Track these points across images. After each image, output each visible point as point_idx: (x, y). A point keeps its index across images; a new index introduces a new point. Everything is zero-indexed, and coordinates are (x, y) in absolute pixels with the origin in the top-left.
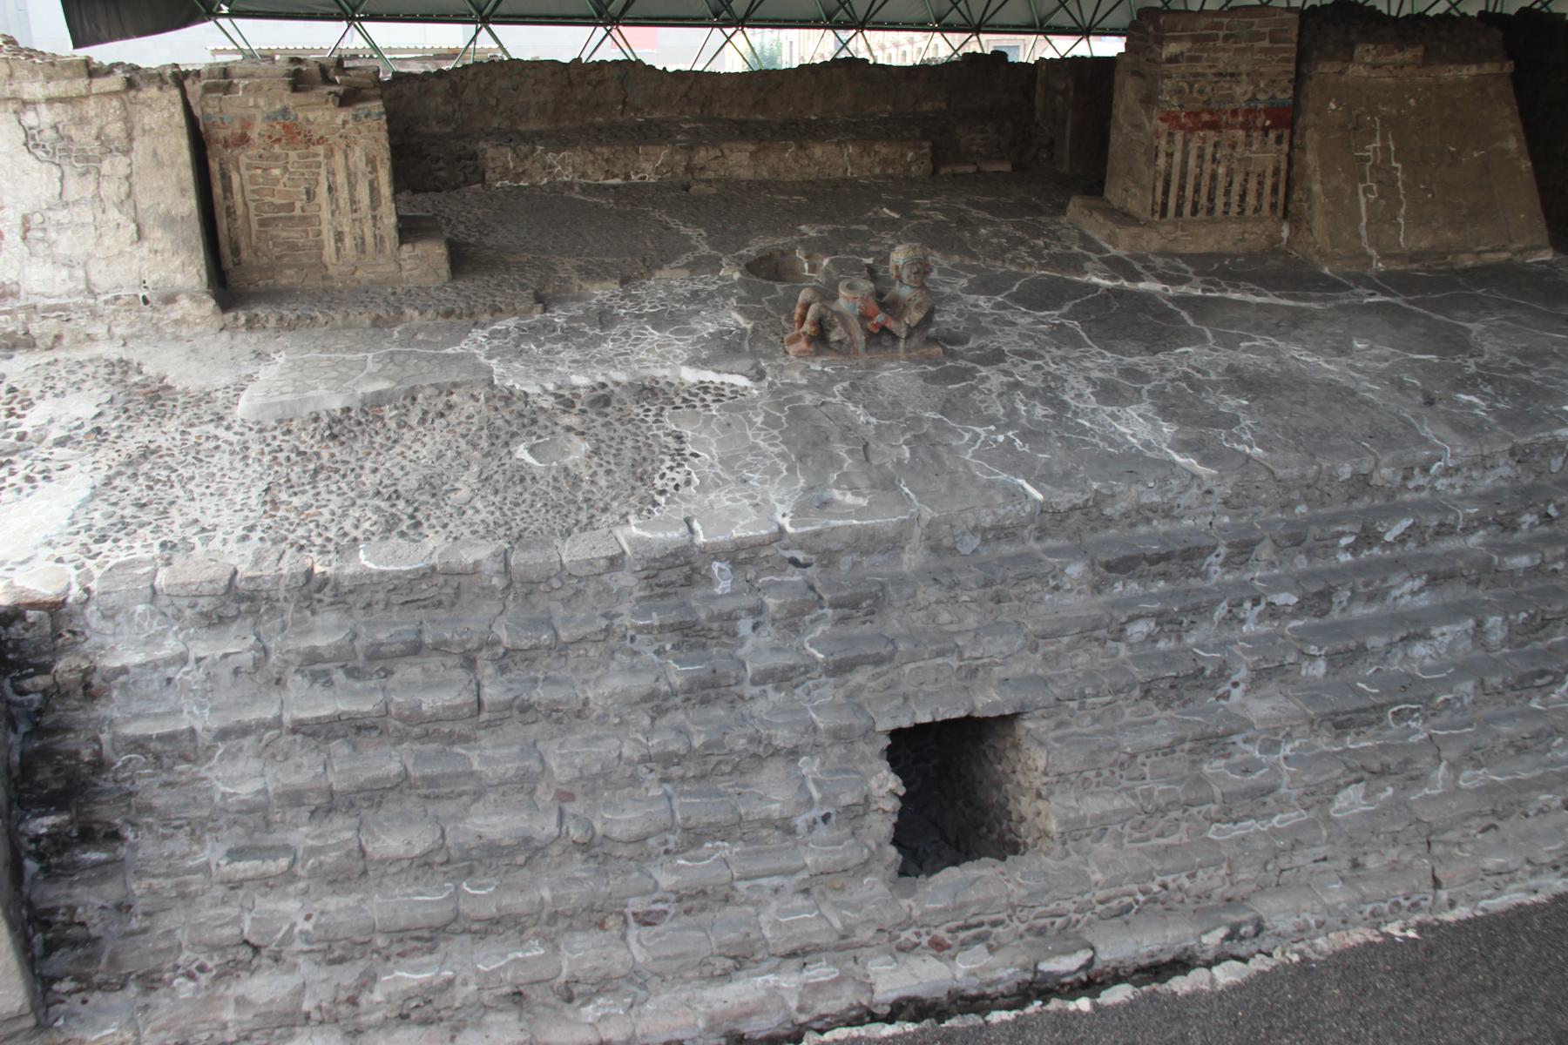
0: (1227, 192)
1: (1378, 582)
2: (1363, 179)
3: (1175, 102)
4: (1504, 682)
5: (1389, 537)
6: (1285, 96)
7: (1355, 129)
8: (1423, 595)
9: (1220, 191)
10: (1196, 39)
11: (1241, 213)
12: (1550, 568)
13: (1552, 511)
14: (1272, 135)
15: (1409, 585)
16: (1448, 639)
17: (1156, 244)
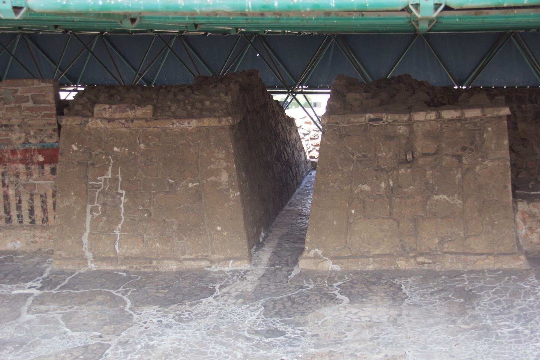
0: (19, 208)
2: (92, 202)
7: (92, 164)
9: (13, 206)
11: (33, 222)
14: (47, 168)
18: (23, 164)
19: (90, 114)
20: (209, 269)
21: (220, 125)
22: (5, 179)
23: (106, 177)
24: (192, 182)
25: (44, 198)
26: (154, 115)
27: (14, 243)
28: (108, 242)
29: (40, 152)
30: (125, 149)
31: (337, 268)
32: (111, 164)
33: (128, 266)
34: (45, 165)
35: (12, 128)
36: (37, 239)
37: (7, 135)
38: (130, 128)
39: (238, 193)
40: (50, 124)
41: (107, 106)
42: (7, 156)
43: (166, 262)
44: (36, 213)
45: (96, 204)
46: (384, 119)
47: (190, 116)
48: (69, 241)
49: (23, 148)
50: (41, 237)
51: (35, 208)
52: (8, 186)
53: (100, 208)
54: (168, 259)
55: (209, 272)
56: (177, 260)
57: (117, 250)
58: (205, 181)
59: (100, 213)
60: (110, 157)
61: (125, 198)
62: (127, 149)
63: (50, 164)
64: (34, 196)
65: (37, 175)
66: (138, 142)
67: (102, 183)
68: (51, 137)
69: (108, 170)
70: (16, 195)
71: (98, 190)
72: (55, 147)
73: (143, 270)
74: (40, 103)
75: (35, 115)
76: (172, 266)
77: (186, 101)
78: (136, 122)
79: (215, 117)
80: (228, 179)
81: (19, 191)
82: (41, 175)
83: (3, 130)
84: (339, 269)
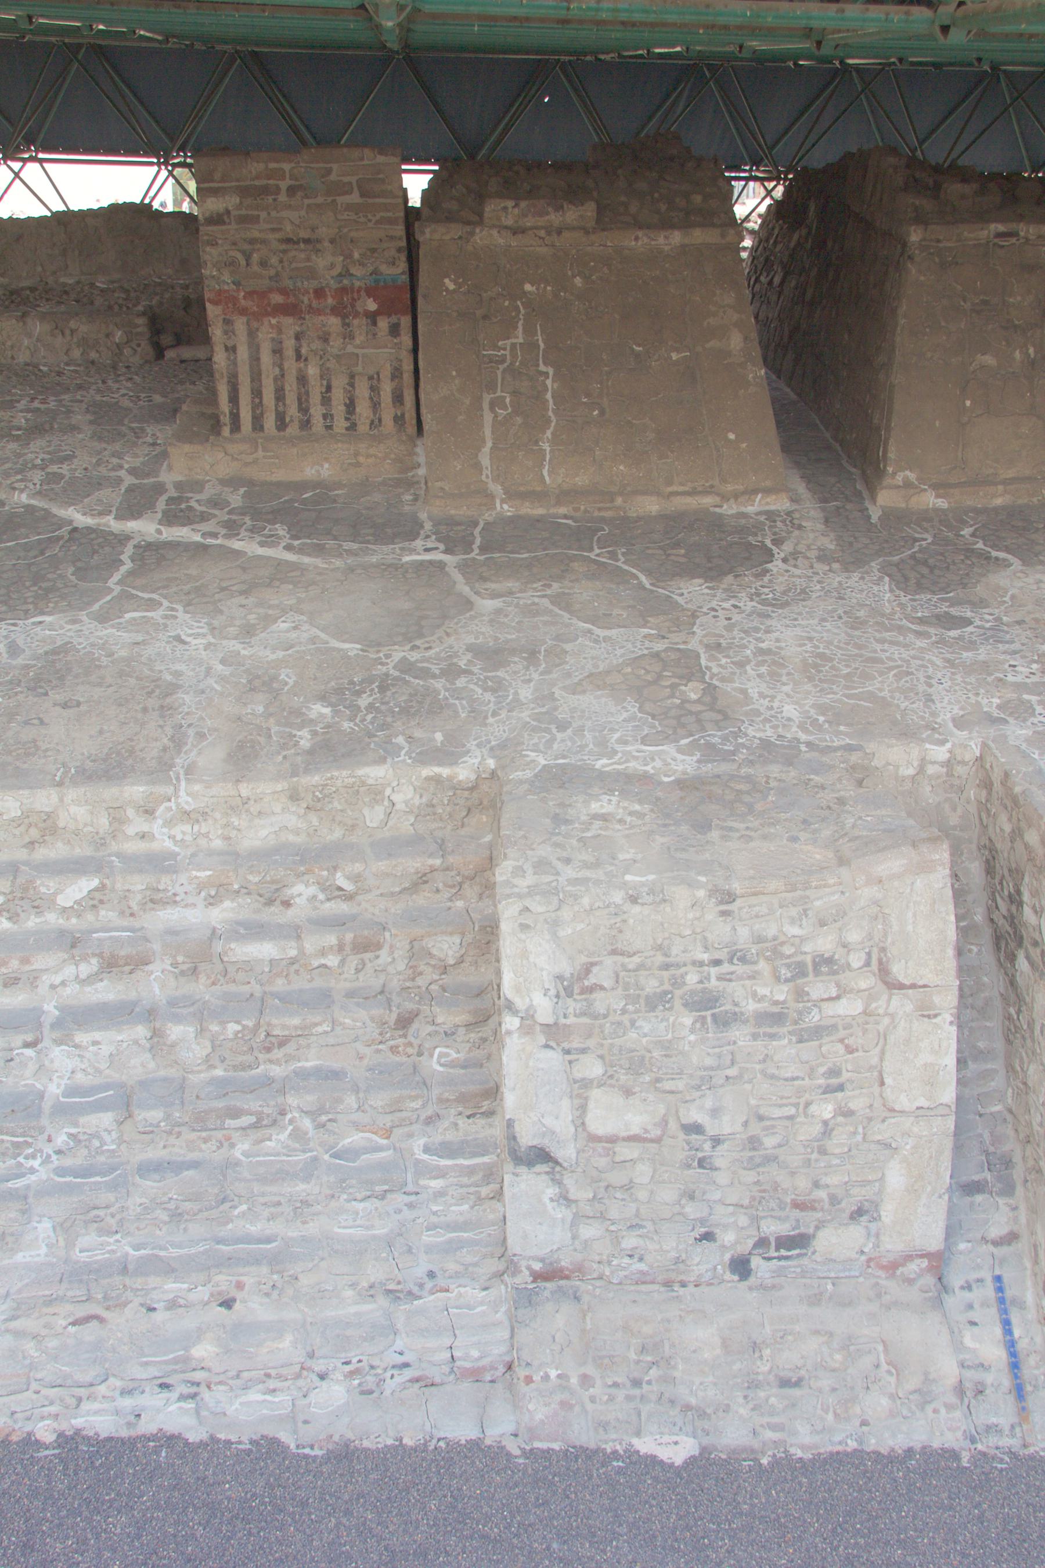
0: (326, 401)
1: (15, 964)
3: (227, 277)
4: (168, 1117)
5: (63, 901)
6: (397, 271)
7: (485, 317)
8: (100, 985)
9: (315, 398)
10: (244, 192)
11: (353, 427)
12: (316, 963)
13: (341, 881)
14: (383, 323)
15: (70, 971)
16: (106, 1050)
17: (226, 468)
18: (337, 315)
19: (476, 218)
20: (717, 510)
21: (723, 242)
22: (301, 346)
23: (514, 341)
24: (678, 350)
25: (375, 382)
26: (598, 221)
27: (317, 467)
28: (530, 463)
29: (371, 292)
30: (545, 288)
31: (942, 503)
32: (521, 317)
33: (570, 508)
34: (379, 318)
35: (318, 246)
36: (361, 459)
37: (308, 259)
38: (553, 246)
39: (763, 372)
40: (392, 238)
41: (510, 204)
42: (306, 301)
43: (640, 498)
44: (358, 410)
45: (499, 393)
46: (1022, 234)
47: (666, 225)
48: (455, 463)
49: (338, 286)
50: (368, 456)
51: (356, 401)
52: (306, 360)
53: (508, 400)
54: (645, 493)
55: (721, 516)
56: (659, 494)
57: (547, 478)
58: (699, 349)
59: (510, 410)
60: (519, 303)
61: (553, 381)
62: (549, 288)
63: (390, 316)
64: (357, 377)
65: (362, 338)
66: (570, 273)
67: (507, 353)
68: (394, 264)
69: (517, 327)
70: (322, 377)
71: (501, 367)
72: (399, 282)
73: (596, 514)
74: (375, 197)
75: (362, 220)
76: (651, 506)
77: (656, 195)
78: (566, 234)
79: (713, 225)
80: (742, 345)
81: (328, 369)
82: (370, 337)
83: (302, 251)
84: (945, 506)
